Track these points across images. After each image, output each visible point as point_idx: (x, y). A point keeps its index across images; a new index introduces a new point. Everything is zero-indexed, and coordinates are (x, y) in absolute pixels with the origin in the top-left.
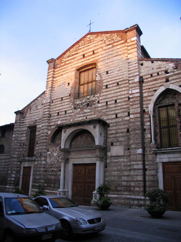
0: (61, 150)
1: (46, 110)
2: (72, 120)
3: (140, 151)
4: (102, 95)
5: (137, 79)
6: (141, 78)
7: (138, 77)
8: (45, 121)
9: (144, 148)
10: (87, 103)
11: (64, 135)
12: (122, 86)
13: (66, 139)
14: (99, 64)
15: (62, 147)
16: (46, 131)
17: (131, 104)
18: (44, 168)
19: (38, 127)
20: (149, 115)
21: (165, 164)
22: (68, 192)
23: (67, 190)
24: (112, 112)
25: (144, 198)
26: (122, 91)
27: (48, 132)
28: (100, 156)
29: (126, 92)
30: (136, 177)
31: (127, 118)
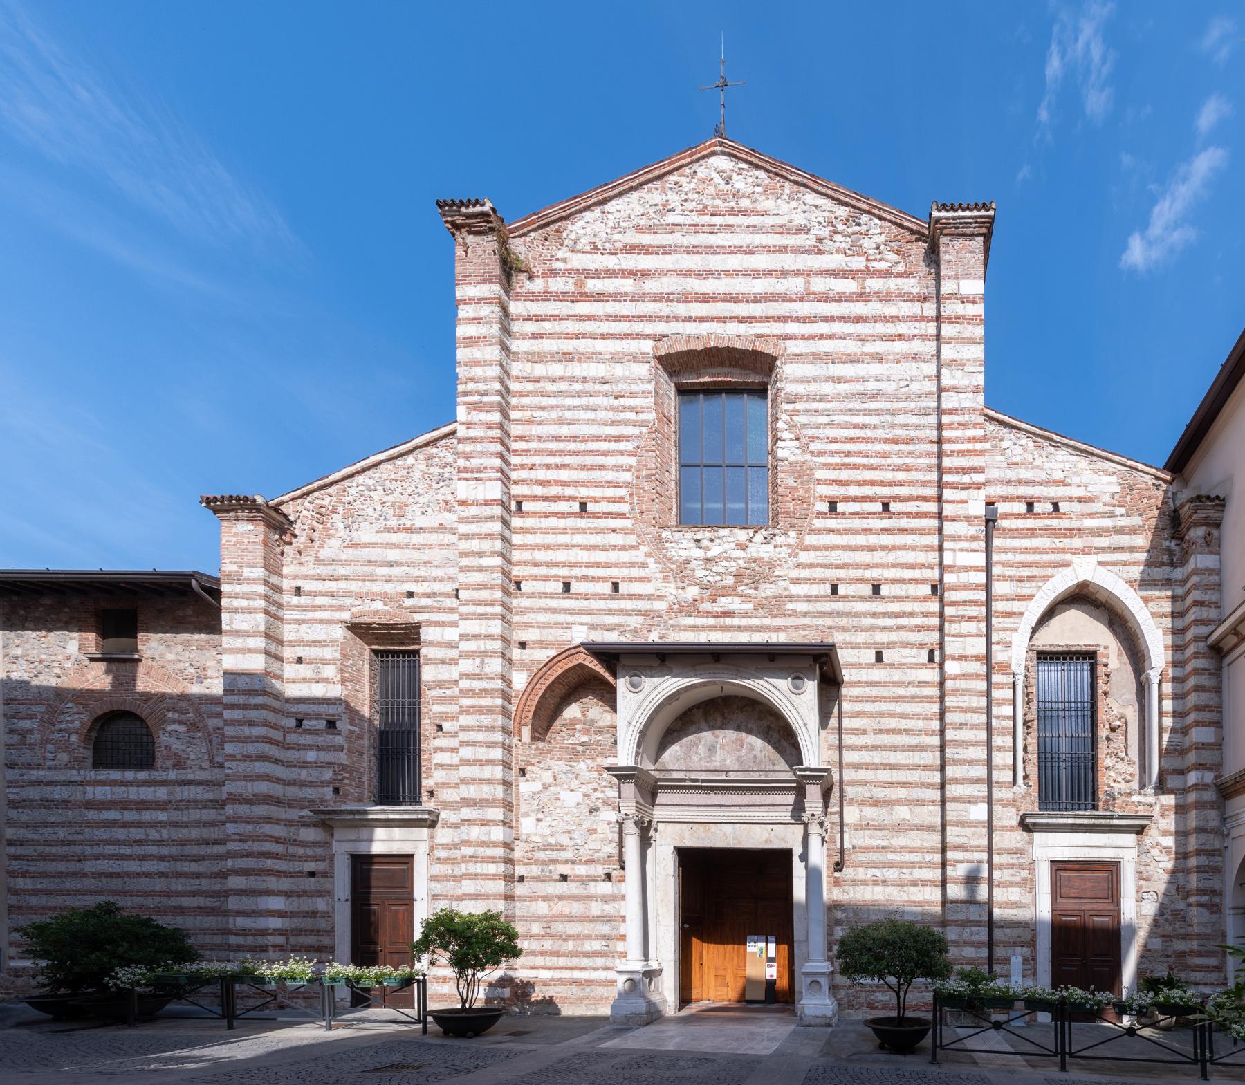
4: (810, 539)
10: (733, 563)
12: (904, 523)
24: (861, 637)
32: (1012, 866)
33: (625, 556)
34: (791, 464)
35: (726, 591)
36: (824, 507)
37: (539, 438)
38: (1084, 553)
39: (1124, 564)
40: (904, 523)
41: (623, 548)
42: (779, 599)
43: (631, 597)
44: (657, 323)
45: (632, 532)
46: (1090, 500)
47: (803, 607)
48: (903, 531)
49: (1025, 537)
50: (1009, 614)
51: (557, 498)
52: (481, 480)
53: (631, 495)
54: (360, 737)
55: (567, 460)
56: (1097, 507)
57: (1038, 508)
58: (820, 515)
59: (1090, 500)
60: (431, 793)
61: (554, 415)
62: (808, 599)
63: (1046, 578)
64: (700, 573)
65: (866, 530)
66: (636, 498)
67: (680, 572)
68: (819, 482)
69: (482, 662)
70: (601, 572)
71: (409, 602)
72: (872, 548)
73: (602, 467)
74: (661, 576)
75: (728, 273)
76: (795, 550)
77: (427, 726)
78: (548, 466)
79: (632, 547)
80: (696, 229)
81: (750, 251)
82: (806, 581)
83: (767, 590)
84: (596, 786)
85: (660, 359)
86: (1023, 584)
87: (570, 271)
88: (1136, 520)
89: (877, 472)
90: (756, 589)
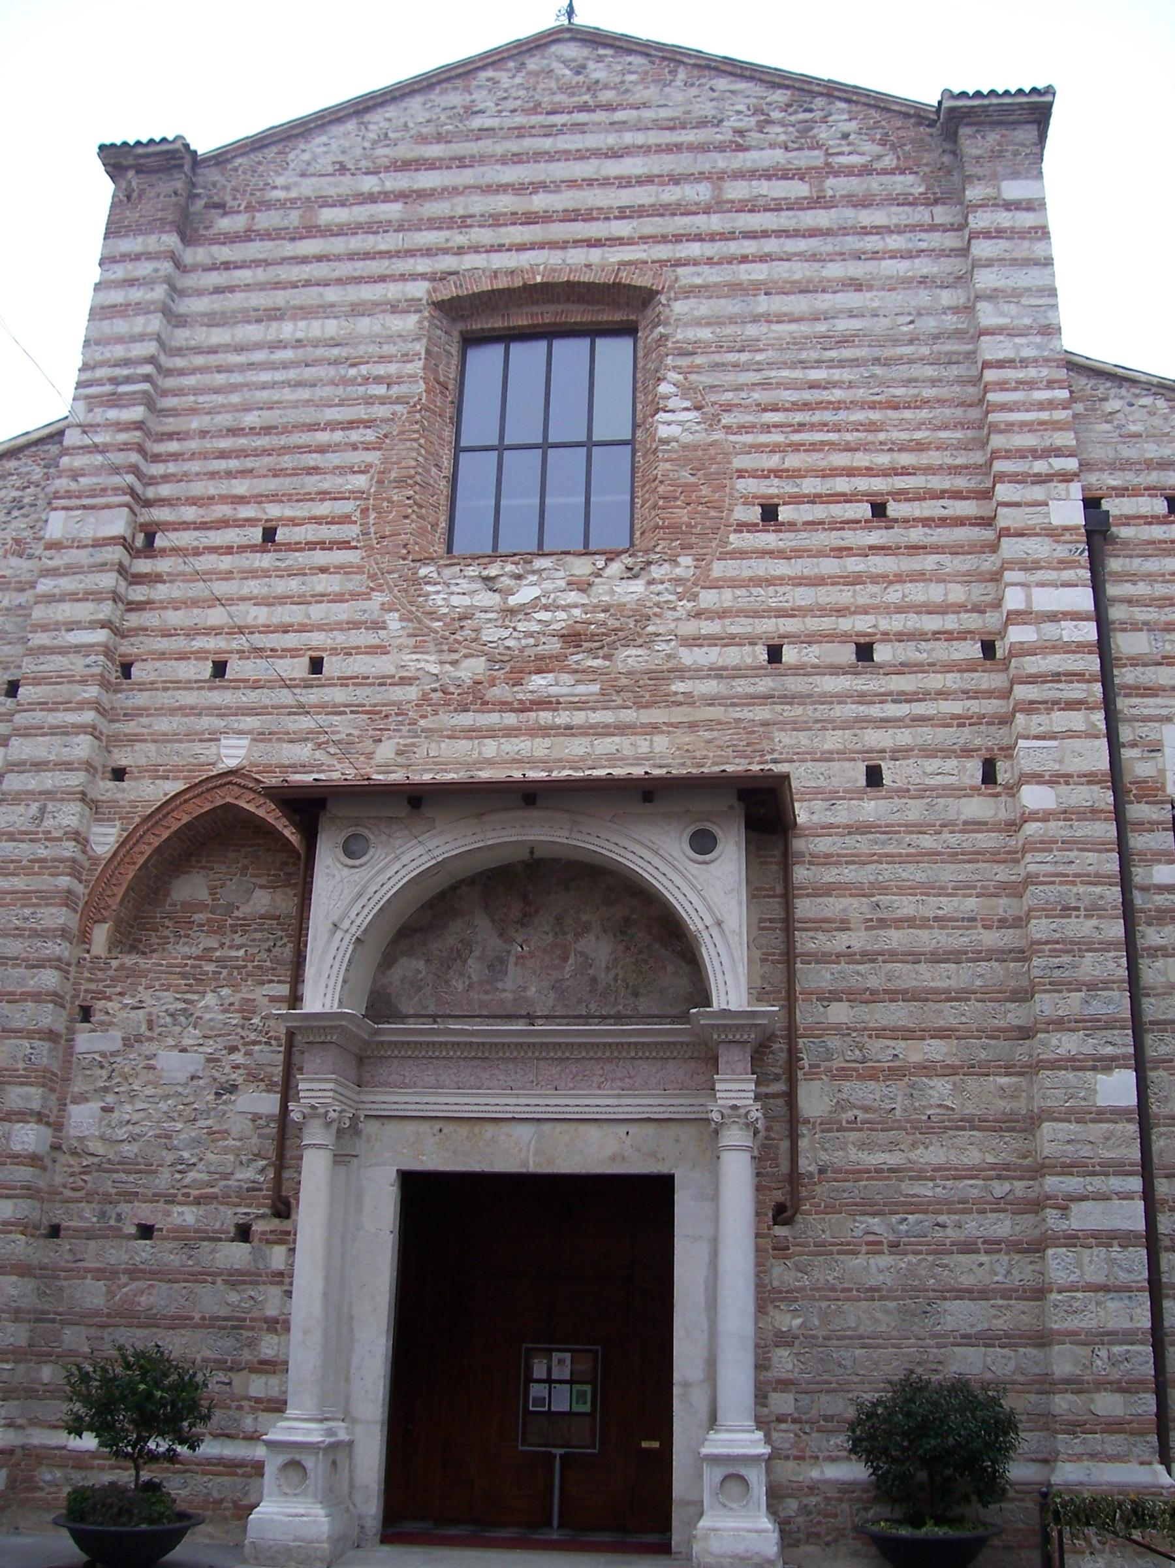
1: (84, 611)
4: (718, 569)
5: (1069, 512)
8: (72, 718)
10: (562, 615)
16: (70, 815)
18: (31, 1192)
24: (833, 740)
27: (89, 827)
30: (1092, 1307)
33: (342, 612)
34: (685, 447)
37: (204, 434)
41: (339, 598)
43: (344, 681)
44: (440, 257)
45: (359, 570)
48: (915, 549)
51: (223, 524)
52: (93, 507)
53: (365, 511)
55: (249, 463)
58: (742, 527)
61: (235, 398)
62: (718, 672)
64: (490, 634)
66: (373, 515)
67: (454, 635)
68: (741, 474)
69: (43, 810)
70: (291, 640)
72: (855, 580)
75: (572, 184)
76: (687, 589)
78: (213, 475)
79: (355, 596)
80: (520, 132)
81: (614, 154)
82: (712, 640)
83: (631, 658)
84: (233, 1040)
85: (439, 305)
87: (293, 201)
89: (859, 455)
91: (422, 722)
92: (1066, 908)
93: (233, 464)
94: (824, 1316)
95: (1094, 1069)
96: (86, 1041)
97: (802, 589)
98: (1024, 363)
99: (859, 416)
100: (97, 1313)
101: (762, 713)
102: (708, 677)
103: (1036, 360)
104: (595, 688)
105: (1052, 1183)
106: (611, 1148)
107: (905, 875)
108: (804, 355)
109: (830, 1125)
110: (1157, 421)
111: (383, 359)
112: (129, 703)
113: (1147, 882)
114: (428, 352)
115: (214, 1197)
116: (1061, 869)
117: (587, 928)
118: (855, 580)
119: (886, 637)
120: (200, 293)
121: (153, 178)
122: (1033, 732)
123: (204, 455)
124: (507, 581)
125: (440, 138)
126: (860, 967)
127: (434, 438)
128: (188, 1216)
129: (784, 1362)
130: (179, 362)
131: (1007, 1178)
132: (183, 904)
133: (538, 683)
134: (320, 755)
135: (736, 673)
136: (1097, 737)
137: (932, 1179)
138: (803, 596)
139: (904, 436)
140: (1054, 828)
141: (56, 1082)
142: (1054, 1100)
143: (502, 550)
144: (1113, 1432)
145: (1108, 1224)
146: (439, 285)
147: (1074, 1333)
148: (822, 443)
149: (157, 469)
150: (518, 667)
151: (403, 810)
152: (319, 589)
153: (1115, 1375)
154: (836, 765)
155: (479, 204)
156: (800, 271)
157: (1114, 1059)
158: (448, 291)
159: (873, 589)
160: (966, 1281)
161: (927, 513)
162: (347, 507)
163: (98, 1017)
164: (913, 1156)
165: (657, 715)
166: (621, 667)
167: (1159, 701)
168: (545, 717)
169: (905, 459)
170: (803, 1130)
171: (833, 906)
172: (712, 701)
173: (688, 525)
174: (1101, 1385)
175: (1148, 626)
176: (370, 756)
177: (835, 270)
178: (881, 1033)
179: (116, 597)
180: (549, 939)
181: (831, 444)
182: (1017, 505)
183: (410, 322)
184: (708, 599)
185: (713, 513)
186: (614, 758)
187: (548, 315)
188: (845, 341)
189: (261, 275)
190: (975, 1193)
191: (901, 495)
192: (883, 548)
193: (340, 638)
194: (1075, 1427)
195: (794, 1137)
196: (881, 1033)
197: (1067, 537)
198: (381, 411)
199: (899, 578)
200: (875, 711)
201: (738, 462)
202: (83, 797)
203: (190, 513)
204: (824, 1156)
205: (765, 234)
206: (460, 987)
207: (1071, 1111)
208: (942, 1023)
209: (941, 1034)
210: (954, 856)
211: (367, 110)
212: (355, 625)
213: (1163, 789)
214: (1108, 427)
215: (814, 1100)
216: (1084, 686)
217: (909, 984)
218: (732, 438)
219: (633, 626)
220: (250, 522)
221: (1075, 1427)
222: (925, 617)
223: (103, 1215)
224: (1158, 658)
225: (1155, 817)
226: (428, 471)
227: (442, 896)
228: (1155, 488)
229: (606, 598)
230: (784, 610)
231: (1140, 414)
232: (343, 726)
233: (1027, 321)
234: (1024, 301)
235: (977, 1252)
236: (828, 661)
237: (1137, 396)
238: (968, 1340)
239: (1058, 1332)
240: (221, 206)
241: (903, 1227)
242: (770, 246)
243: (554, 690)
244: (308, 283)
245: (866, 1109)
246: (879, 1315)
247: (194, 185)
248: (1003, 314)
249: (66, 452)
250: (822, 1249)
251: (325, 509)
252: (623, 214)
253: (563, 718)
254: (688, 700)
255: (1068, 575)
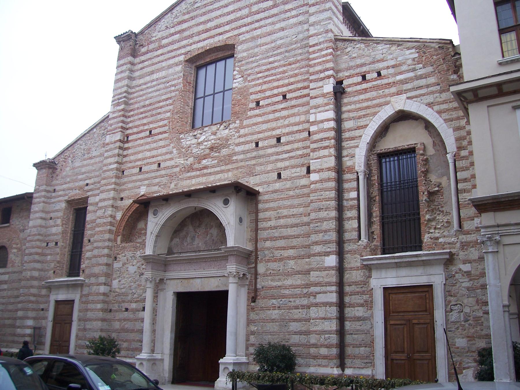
0: (147, 259)
1: (112, 160)
2: (172, 186)
3: (332, 261)
4: (245, 123)
5: (329, 87)
6: (340, 83)
7: (332, 80)
9: (341, 254)
10: (210, 142)
11: (154, 223)
12: (294, 102)
13: (157, 231)
14: (239, 48)
15: (149, 251)
16: (109, 212)
17: (313, 146)
18: (104, 302)
19: (91, 200)
20: (356, 174)
21: (390, 291)
22: (162, 360)
23: (159, 356)
24: (270, 167)
25: (341, 372)
26: (294, 115)
28: (238, 273)
29: (303, 118)
30: (321, 324)
31: (304, 182)
32: (358, 293)
33: (164, 150)
34: (239, 89)
35: (205, 157)
36: (254, 105)
37: (138, 108)
38: (398, 94)
39: (423, 95)
40: (294, 102)
41: (164, 147)
42: (230, 156)
46: (400, 65)
47: (242, 157)
49: (361, 94)
50: (353, 139)
53: (169, 122)
54: (65, 248)
55: (147, 114)
56: (404, 68)
57: (368, 77)
59: (400, 65)
60: (83, 271)
61: (144, 97)
62: (244, 152)
63: (375, 114)
65: (274, 111)
66: (171, 123)
67: (185, 152)
71: (86, 188)
72: (277, 119)
73: (159, 113)
74: (178, 156)
75: (216, 18)
77: (85, 240)
78: (140, 119)
86: (361, 120)
88: (430, 69)
90: (219, 152)
91: (180, 177)
92: (320, 209)
93: (144, 115)
94: (262, 326)
95: (325, 255)
96: (116, 265)
97: (264, 124)
98: (320, 43)
99: (281, 70)
100: (117, 330)
101: (253, 162)
102: (241, 154)
103: (323, 42)
104: (216, 161)
105: (313, 289)
106: (216, 284)
107: (285, 203)
108: (268, 55)
109: (265, 275)
110: (361, 52)
111: (174, 79)
112: (124, 181)
113: (348, 198)
114: (184, 75)
115: (139, 301)
116: (319, 197)
117: (212, 227)
118: (277, 119)
119: (284, 135)
120: (138, 70)
121: (126, 42)
122: (314, 158)
123: (137, 114)
124: (198, 135)
125: (188, 13)
126: (273, 231)
127: (187, 99)
128: (134, 306)
129: (252, 339)
130: (133, 90)
131: (307, 288)
132: (140, 229)
133: (204, 162)
134: (160, 189)
135: (248, 151)
136: (331, 156)
137: (289, 289)
138: (264, 127)
139: (292, 73)
140: (318, 186)
141: (108, 275)
142: (314, 265)
143: (214, 123)
144: (324, 359)
145: (326, 300)
146: (186, 55)
147: (316, 331)
148: (272, 80)
149: (129, 120)
150: (200, 158)
151: (164, 202)
152: (160, 145)
153: (326, 343)
154: (270, 174)
155: (196, 30)
156: (269, 29)
157: (330, 252)
158: (189, 56)
159: (281, 121)
160: (296, 317)
161: (296, 95)
162: (166, 122)
163: (118, 259)
164: (284, 282)
165: (229, 167)
166: (222, 155)
167: (355, 141)
168: (205, 171)
169: (292, 80)
170: (258, 277)
171: (267, 214)
172: (242, 161)
173: (239, 112)
174: (322, 346)
175: (354, 118)
176: (169, 187)
177: (278, 26)
178: (277, 249)
179: (119, 155)
180: (204, 230)
181: (273, 80)
182: (315, 89)
183: (179, 68)
184: (242, 132)
185: (244, 107)
186: (219, 180)
187: (213, 56)
188: (279, 47)
189: (150, 62)
190: (299, 292)
191: (290, 91)
192: (285, 108)
193: (164, 157)
194: (315, 357)
195: (256, 279)
196: (277, 249)
197: (328, 96)
198: (173, 94)
199: (289, 116)
200: (280, 157)
201: (251, 91)
202: (112, 206)
203: (135, 130)
204: (263, 284)
205: (261, 20)
206: (186, 245)
207: (318, 268)
208: (293, 245)
209: (292, 248)
210: (298, 196)
211: (173, 9)
212: (167, 153)
213: (355, 168)
214: (347, 57)
215: (261, 268)
216: (329, 141)
217: (285, 234)
218: (250, 84)
219: (224, 143)
220: (147, 130)
221: (315, 357)
222: (294, 127)
223: (119, 306)
224: (356, 128)
225: (351, 177)
226: (184, 108)
227: (182, 222)
228: (359, 73)
229: (220, 136)
230: (260, 131)
231: (356, 50)
232: (164, 180)
233: (322, 30)
234: (322, 24)
235: (299, 309)
236: (269, 144)
237: (356, 45)
238: (296, 333)
239: (312, 331)
240: (142, 45)
241: (281, 302)
242: (262, 23)
243: (207, 163)
244: (159, 62)
245: (273, 270)
246: (275, 326)
247: (136, 41)
248: (315, 29)
249: (110, 120)
250: (262, 309)
251: (161, 123)
252: (228, 23)
253: (209, 171)
254: (237, 161)
255: (327, 108)
